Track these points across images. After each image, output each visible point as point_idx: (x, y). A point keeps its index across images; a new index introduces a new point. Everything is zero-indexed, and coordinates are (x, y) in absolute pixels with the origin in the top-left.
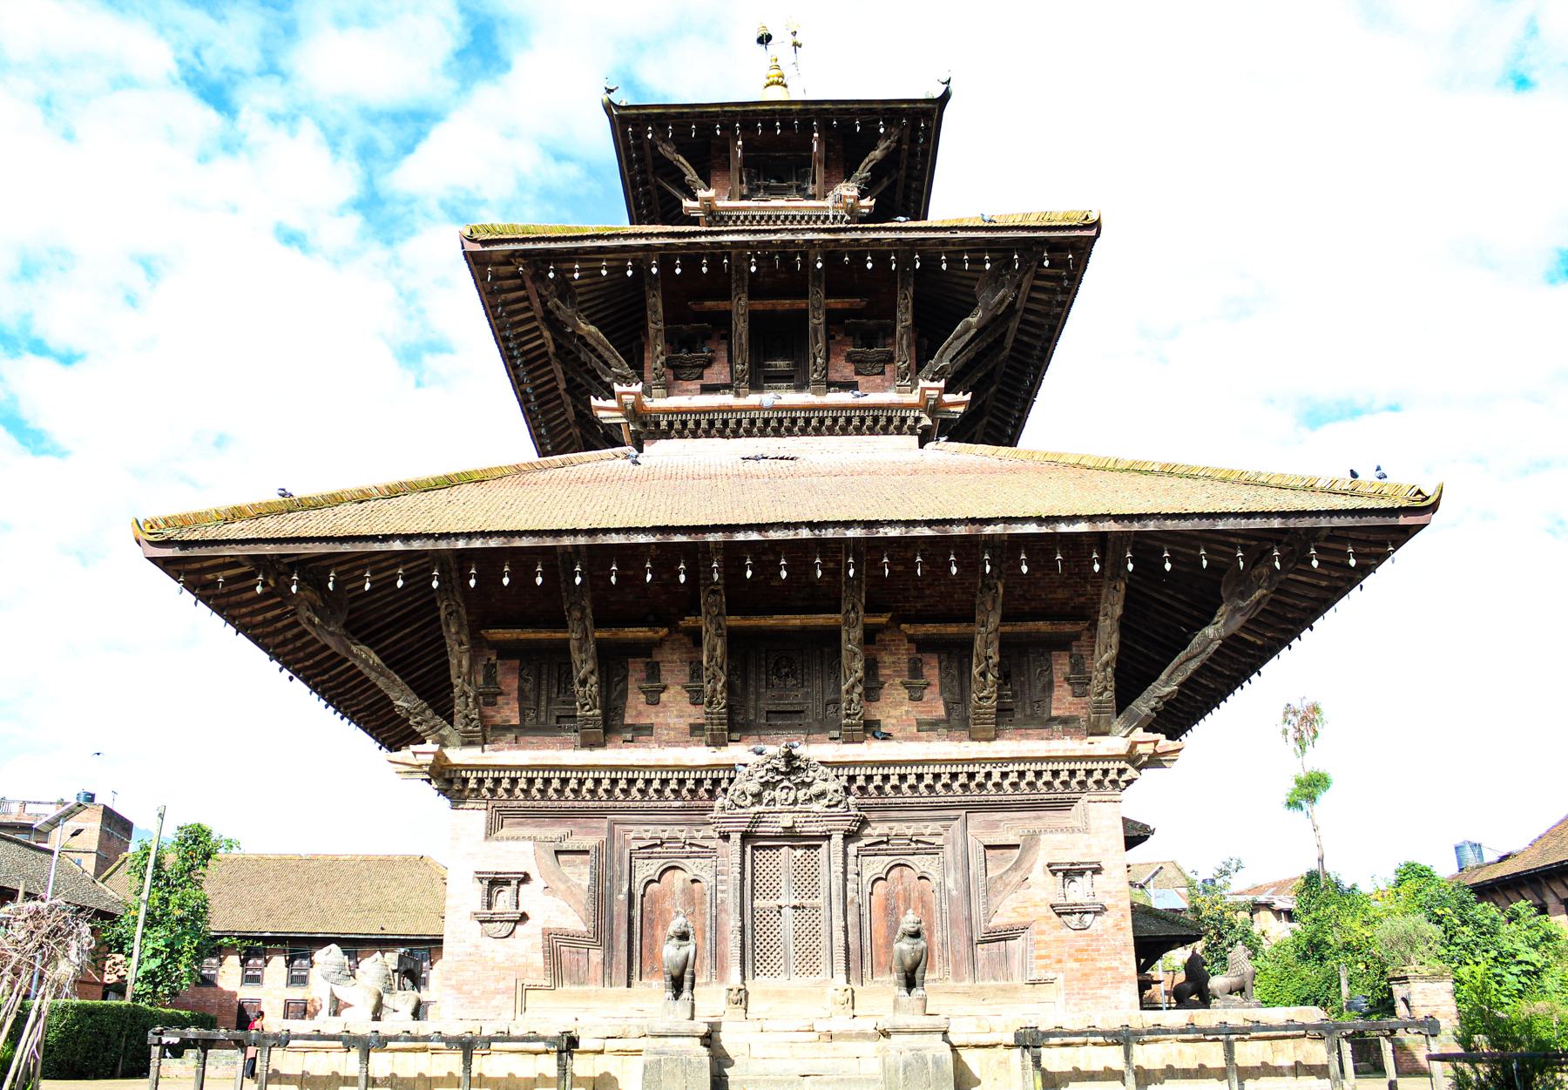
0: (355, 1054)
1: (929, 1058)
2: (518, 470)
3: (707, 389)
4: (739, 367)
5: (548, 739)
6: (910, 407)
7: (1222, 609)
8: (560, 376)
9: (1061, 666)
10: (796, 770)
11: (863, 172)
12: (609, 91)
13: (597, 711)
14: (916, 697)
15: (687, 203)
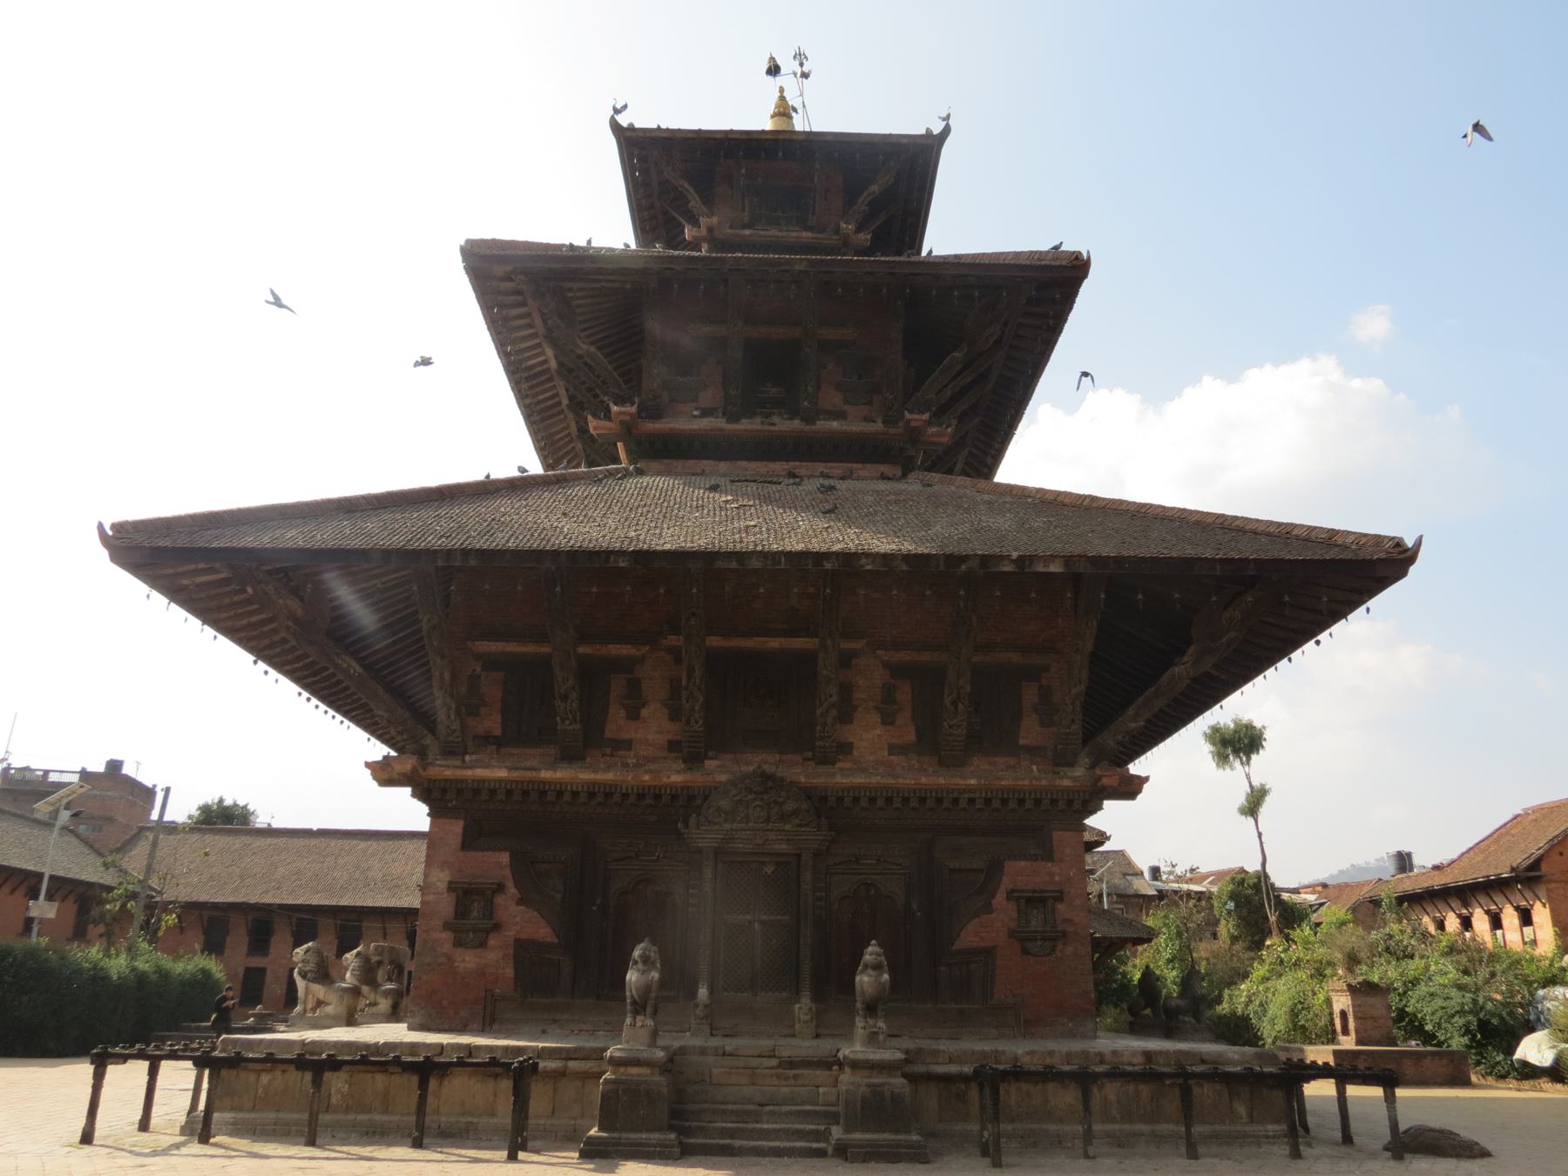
0: (308, 1076)
1: (887, 1094)
5: (528, 751)
7: (1192, 648)
8: (562, 392)
9: (1030, 695)
11: (862, 205)
12: (617, 111)
13: (578, 726)
14: (888, 720)
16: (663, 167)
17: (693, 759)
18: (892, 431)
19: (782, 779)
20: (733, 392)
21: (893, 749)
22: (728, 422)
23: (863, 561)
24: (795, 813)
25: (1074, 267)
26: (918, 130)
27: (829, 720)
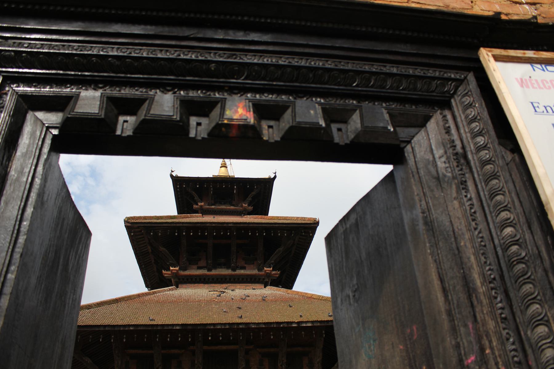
2: (139, 296)
3: (199, 268)
4: (210, 262)
11: (249, 199)
18: (261, 273)
20: (210, 262)
22: (208, 271)
23: (251, 325)
25: (314, 223)
26: (267, 177)
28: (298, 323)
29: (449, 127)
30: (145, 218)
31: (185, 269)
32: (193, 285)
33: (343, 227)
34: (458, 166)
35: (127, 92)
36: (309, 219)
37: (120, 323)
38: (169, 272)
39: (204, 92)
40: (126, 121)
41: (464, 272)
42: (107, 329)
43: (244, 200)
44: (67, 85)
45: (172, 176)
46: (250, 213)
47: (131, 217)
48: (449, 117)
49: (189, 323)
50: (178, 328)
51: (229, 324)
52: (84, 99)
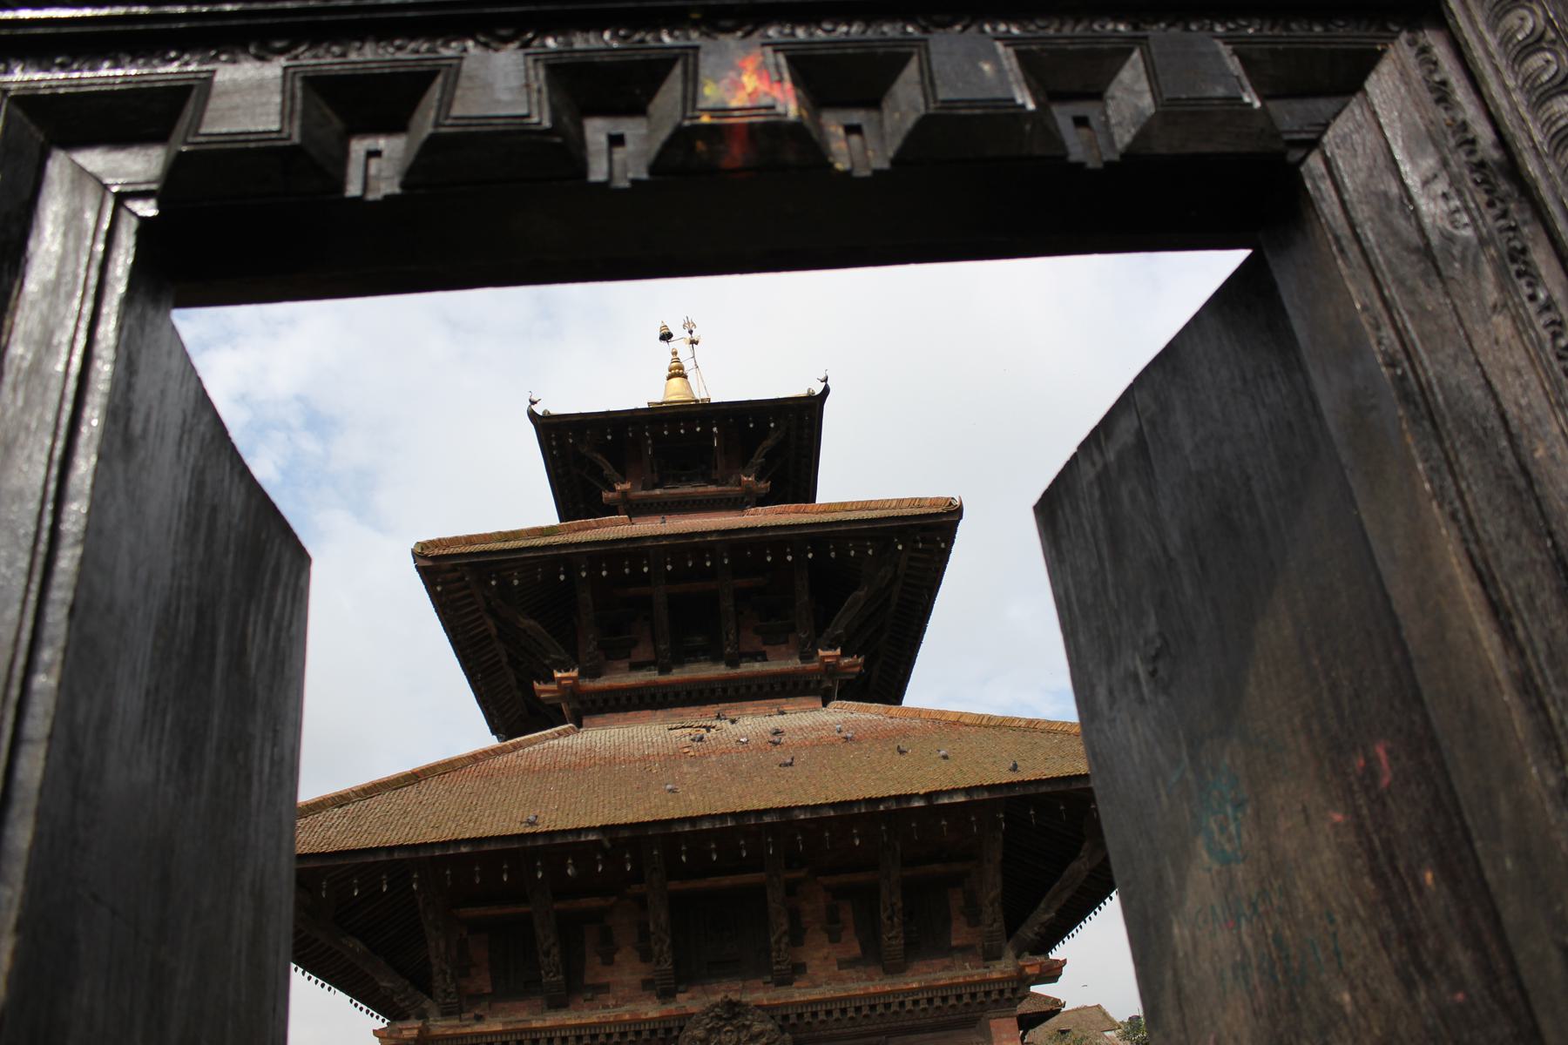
2: (475, 758)
3: (636, 667)
4: (663, 647)
6: (813, 672)
7: (1086, 844)
10: (735, 1016)
11: (758, 460)
12: (533, 403)
14: (834, 938)
15: (607, 495)
16: (579, 450)
17: (666, 995)
18: (809, 666)
19: (747, 1005)
21: (843, 964)
22: (661, 673)
23: (797, 812)
24: (762, 1034)
25: (949, 513)
26: (802, 392)
27: (783, 946)
28: (928, 796)
29: (1444, 83)
30: (470, 540)
31: (595, 674)
32: (621, 716)
33: (1094, 464)
34: (1490, 204)
35: (368, 55)
36: (934, 502)
37: (431, 838)
38: (553, 687)
39: (622, 33)
40: (376, 154)
41: (1555, 544)
42: (396, 856)
43: (744, 463)
44: (167, 52)
45: (532, 415)
46: (762, 501)
47: (431, 542)
48: (1441, 51)
49: (623, 821)
50: (592, 837)
51: (734, 815)
52: (226, 93)
